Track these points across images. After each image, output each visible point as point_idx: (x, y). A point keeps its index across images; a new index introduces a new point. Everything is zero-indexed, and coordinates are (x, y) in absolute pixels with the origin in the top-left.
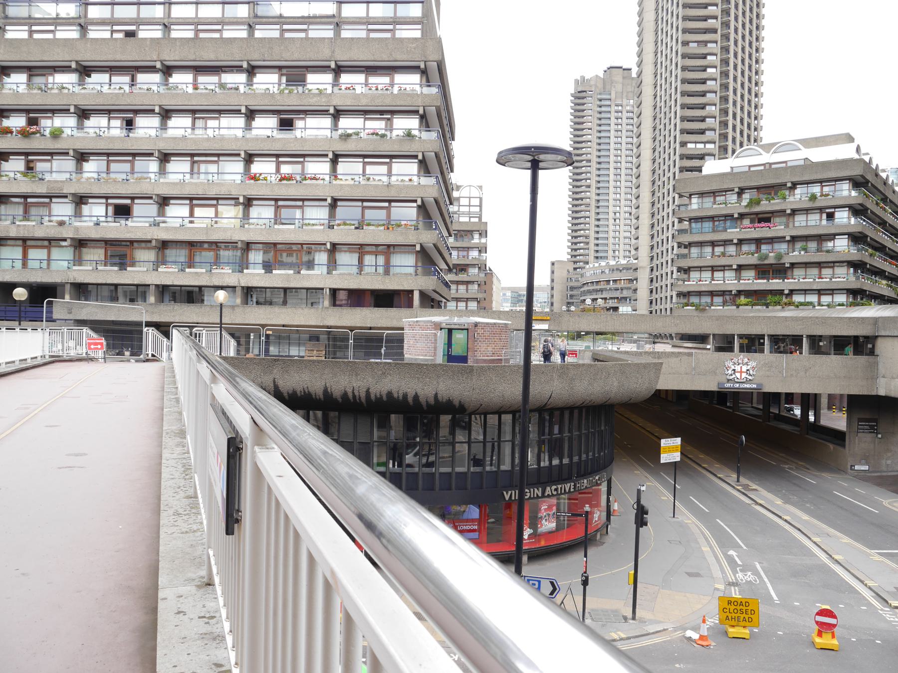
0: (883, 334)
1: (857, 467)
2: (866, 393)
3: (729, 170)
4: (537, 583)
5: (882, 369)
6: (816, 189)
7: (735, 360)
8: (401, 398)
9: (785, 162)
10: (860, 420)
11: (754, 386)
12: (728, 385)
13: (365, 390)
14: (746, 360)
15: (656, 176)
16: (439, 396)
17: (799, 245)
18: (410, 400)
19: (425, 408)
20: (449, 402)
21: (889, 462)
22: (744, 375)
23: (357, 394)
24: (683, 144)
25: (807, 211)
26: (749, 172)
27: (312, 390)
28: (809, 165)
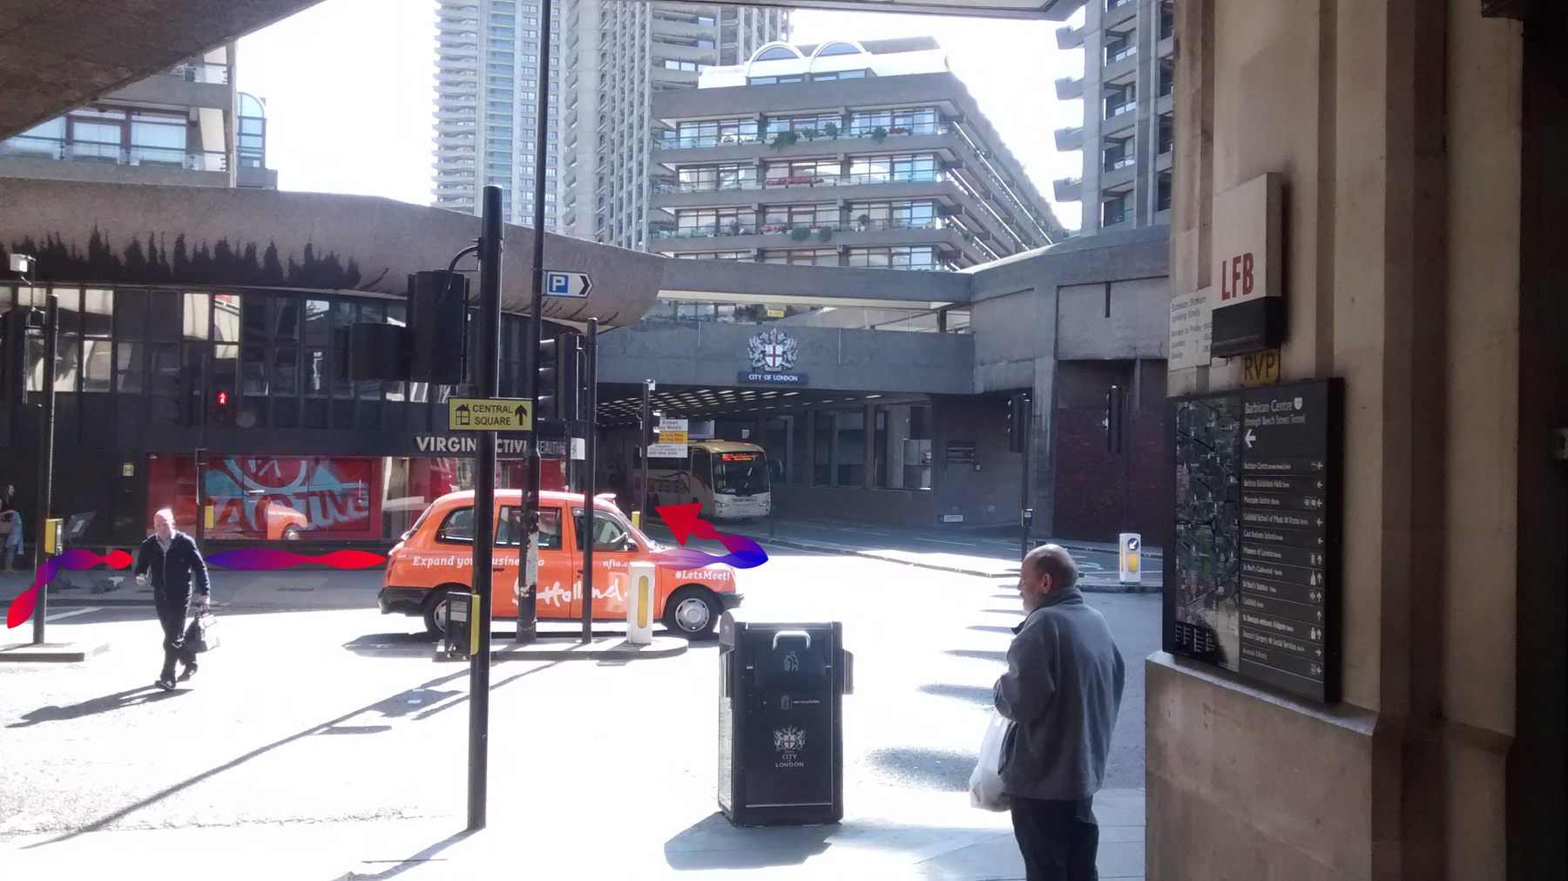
0: (980, 296)
1: (947, 518)
3: (743, 83)
7: (765, 336)
8: (242, 254)
9: (836, 73)
11: (795, 378)
12: (754, 377)
13: (174, 239)
14: (781, 336)
19: (286, 274)
20: (332, 261)
21: (992, 508)
22: (779, 361)
23: (158, 246)
24: (659, 63)
26: (782, 85)
27: (66, 240)
28: (869, 80)
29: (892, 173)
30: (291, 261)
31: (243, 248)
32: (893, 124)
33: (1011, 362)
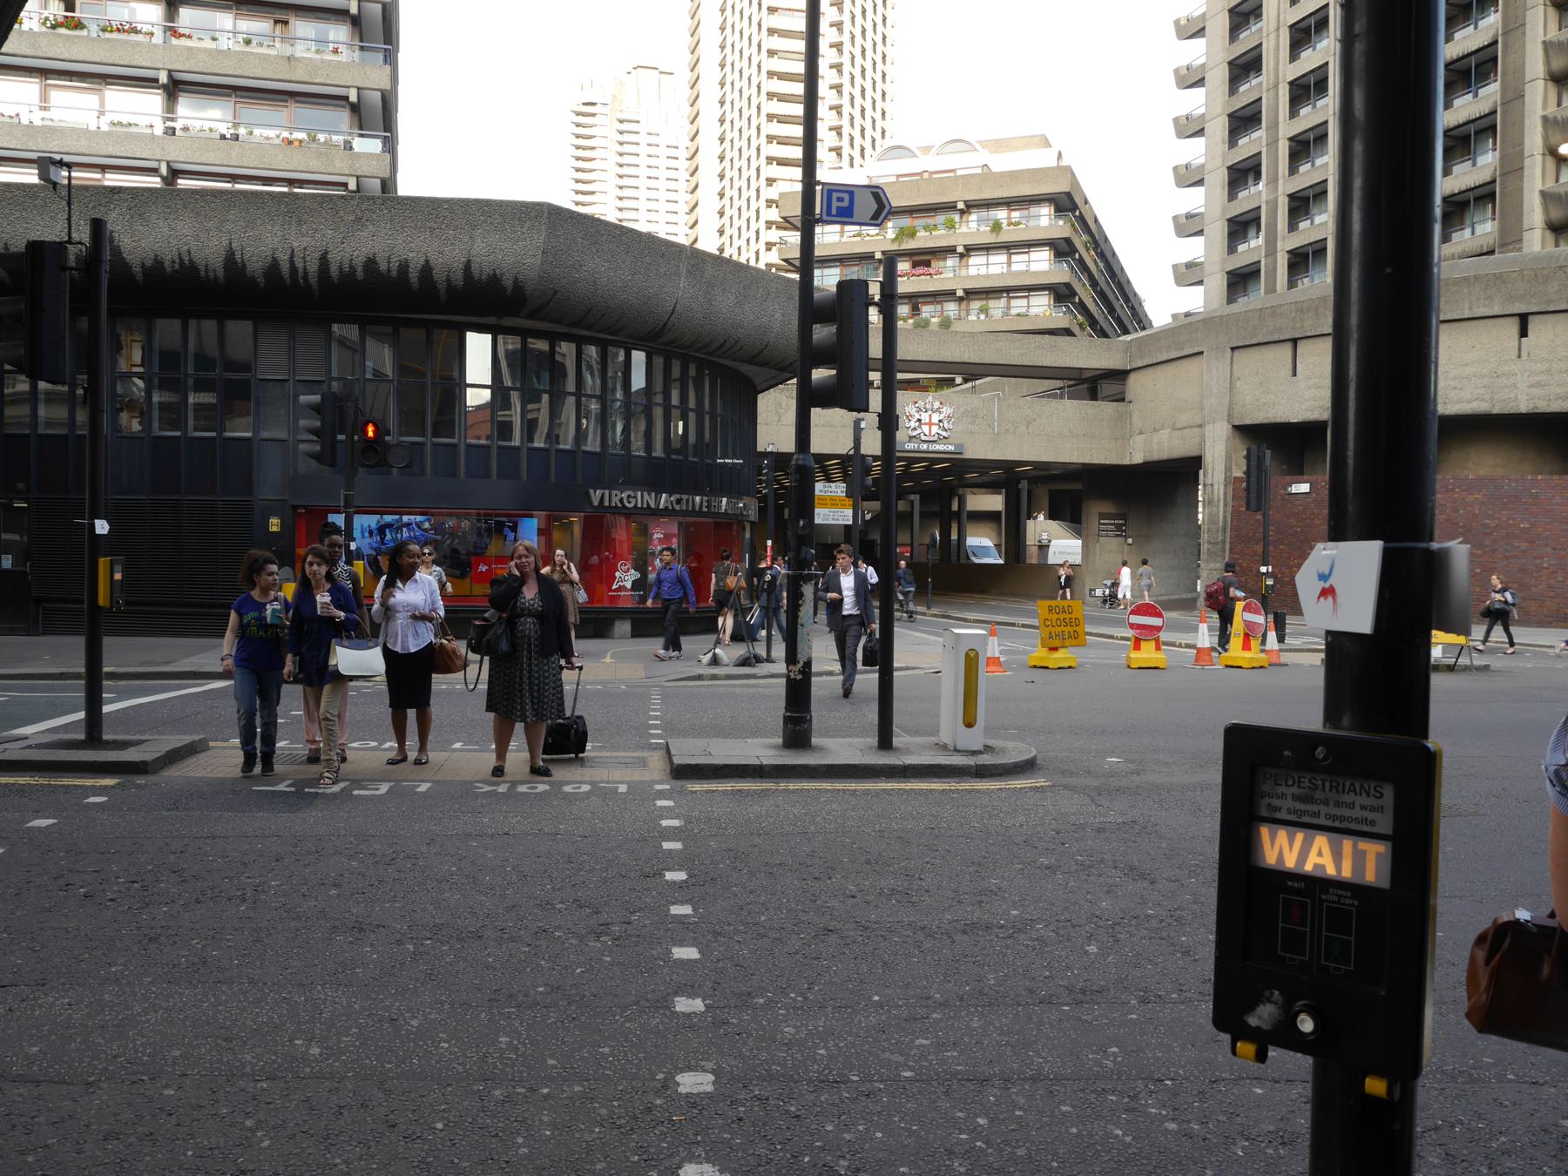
2: (1114, 462)
4: (846, 196)
5: (1138, 423)
6: (1001, 214)
8: (394, 273)
10: (1102, 516)
11: (951, 448)
13: (317, 255)
14: (937, 405)
15: (726, 239)
16: (475, 266)
17: (976, 305)
18: (414, 276)
20: (495, 279)
22: (935, 429)
23: (299, 264)
25: (987, 249)
27: (198, 257)
28: (987, 175)
29: (1009, 263)
30: (448, 280)
31: (395, 266)
32: (1009, 218)
33: (1174, 429)
